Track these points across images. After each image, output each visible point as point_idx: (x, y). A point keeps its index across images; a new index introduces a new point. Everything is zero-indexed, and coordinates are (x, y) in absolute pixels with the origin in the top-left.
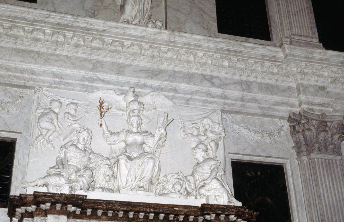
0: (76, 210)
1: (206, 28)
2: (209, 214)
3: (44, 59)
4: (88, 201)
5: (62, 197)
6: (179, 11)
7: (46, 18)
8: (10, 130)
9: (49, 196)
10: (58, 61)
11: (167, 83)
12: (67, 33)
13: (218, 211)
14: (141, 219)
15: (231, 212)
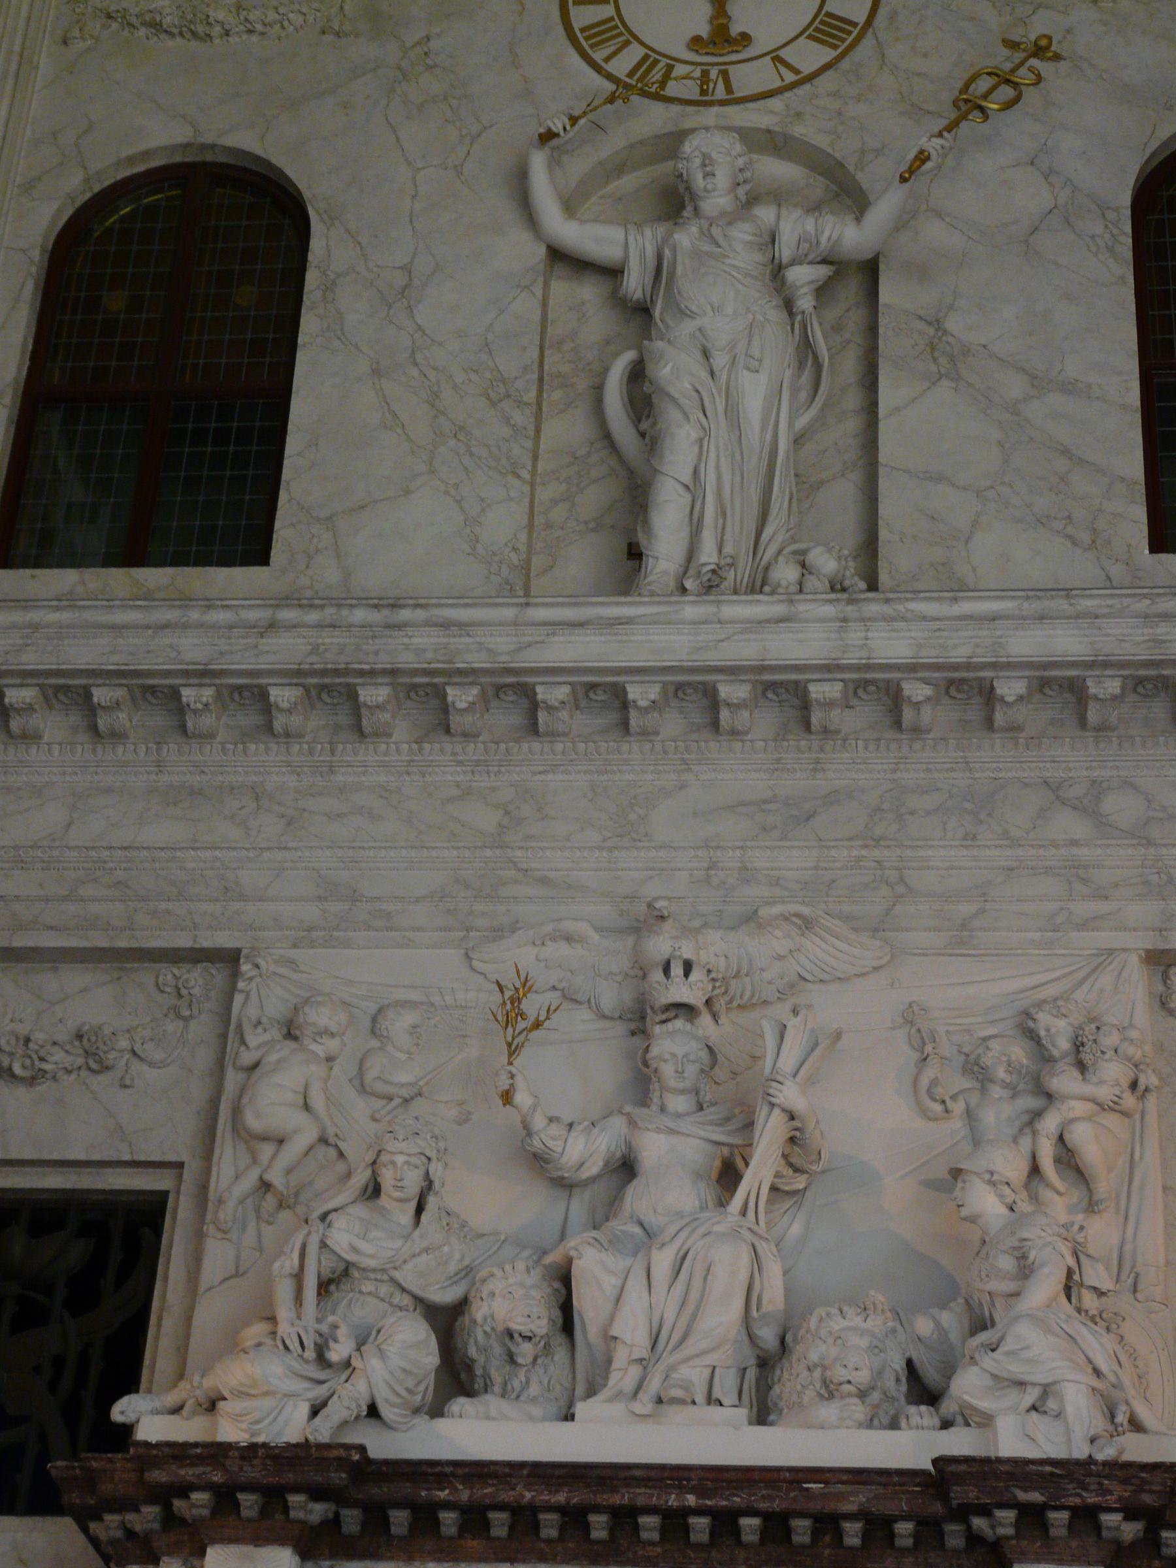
0: (337, 1514)
1: (1086, 538)
2: (985, 1511)
3: (283, 816)
4: (384, 1469)
5: (255, 1457)
6: (940, 478)
7: (262, 635)
8: (136, 1158)
9: (198, 1456)
10: (340, 816)
11: (855, 853)
12: (363, 684)
13: (1025, 1490)
14: (652, 1543)
15: (1097, 1495)
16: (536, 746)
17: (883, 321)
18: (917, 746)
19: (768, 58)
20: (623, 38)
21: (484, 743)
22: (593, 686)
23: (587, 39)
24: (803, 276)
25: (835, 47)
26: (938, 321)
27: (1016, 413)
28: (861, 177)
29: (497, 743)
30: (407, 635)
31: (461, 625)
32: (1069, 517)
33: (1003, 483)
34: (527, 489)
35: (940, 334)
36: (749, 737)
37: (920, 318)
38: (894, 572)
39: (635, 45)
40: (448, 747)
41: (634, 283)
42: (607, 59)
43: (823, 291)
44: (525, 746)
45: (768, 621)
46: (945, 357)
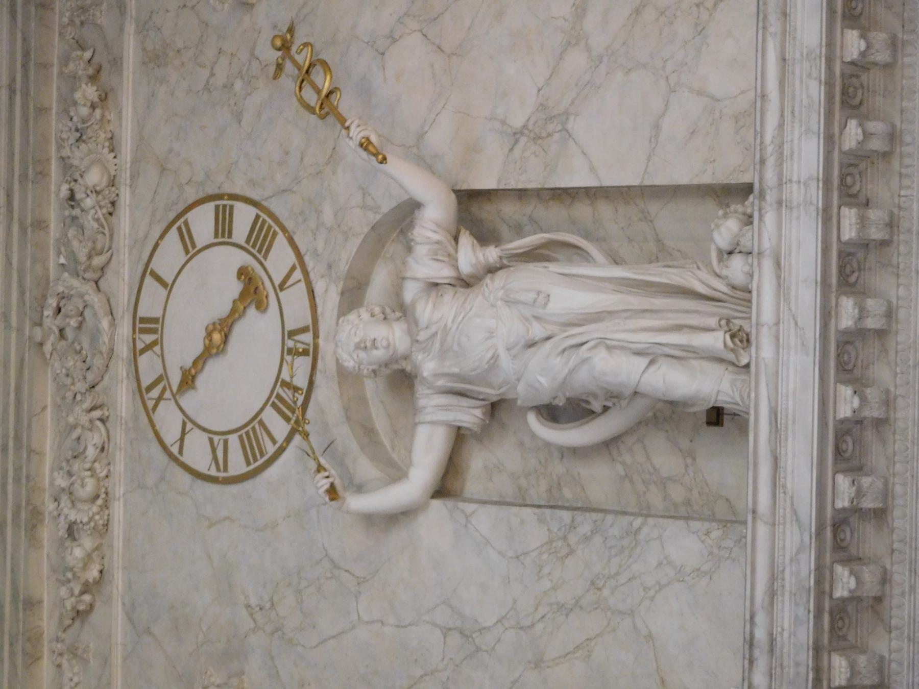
6: (657, 127)
12: (829, 680)
16: (897, 513)
17: (513, 185)
18: (908, 139)
19: (281, 295)
20: (257, 427)
21: (892, 564)
22: (838, 451)
23: (255, 460)
24: (470, 255)
25: (275, 234)
26: (515, 134)
27: (600, 58)
28: (385, 209)
29: (893, 551)
30: (781, 634)
31: (773, 578)
32: (698, 5)
33: (664, 68)
34: (651, 521)
35: (526, 132)
36: (894, 301)
37: (511, 150)
38: (742, 169)
39: (263, 416)
40: (895, 602)
41: (469, 416)
42: (274, 441)
43: (484, 237)
44: (897, 523)
45: (778, 277)
46: (548, 126)
